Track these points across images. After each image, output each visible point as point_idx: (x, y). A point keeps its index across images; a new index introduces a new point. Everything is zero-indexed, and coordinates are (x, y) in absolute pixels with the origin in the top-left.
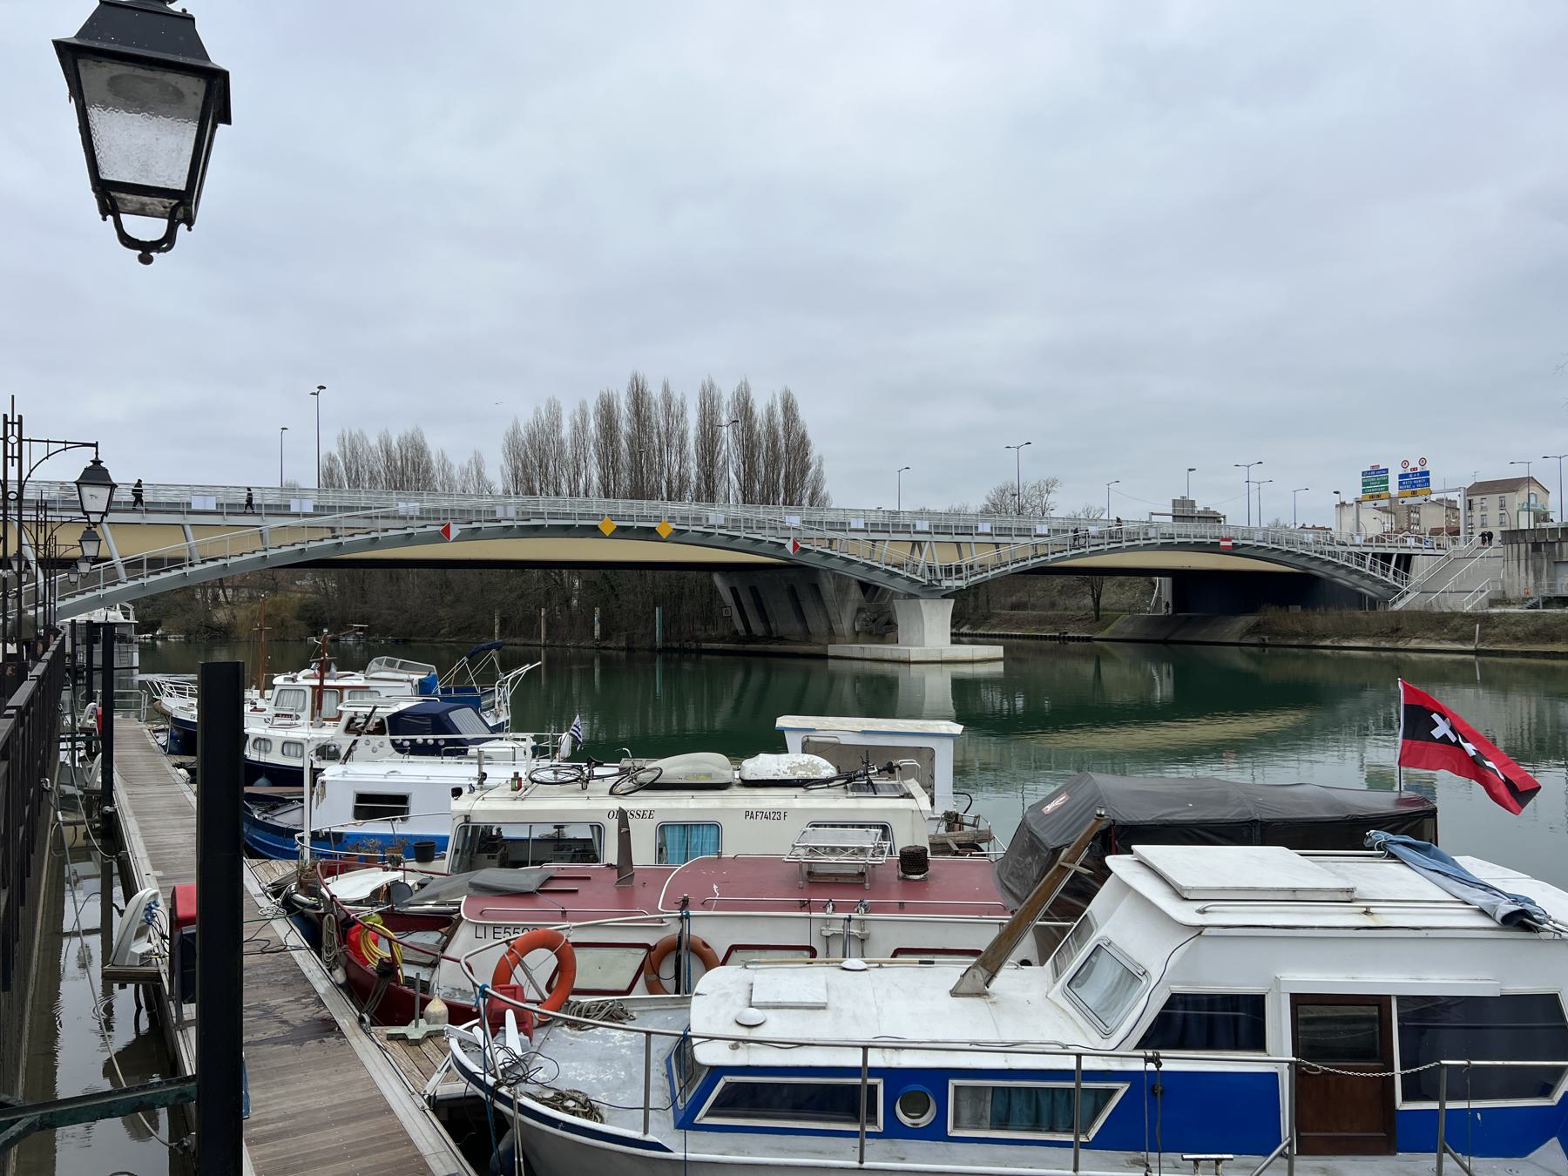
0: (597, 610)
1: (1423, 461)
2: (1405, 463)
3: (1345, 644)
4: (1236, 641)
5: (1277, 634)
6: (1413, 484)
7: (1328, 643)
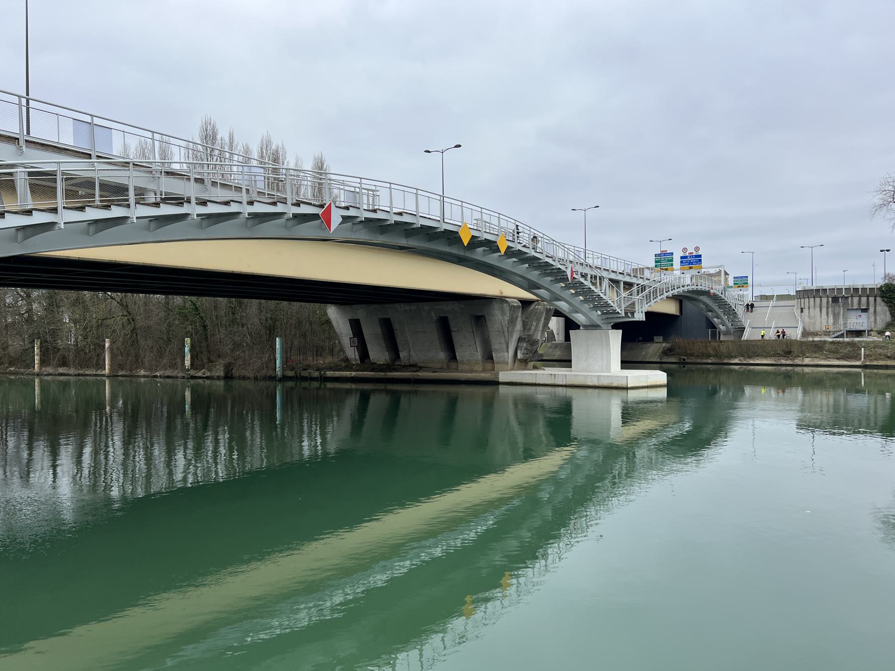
0: (188, 340)
1: (697, 249)
2: (685, 250)
3: (752, 362)
4: (658, 360)
5: (692, 355)
6: (690, 262)
7: (736, 361)
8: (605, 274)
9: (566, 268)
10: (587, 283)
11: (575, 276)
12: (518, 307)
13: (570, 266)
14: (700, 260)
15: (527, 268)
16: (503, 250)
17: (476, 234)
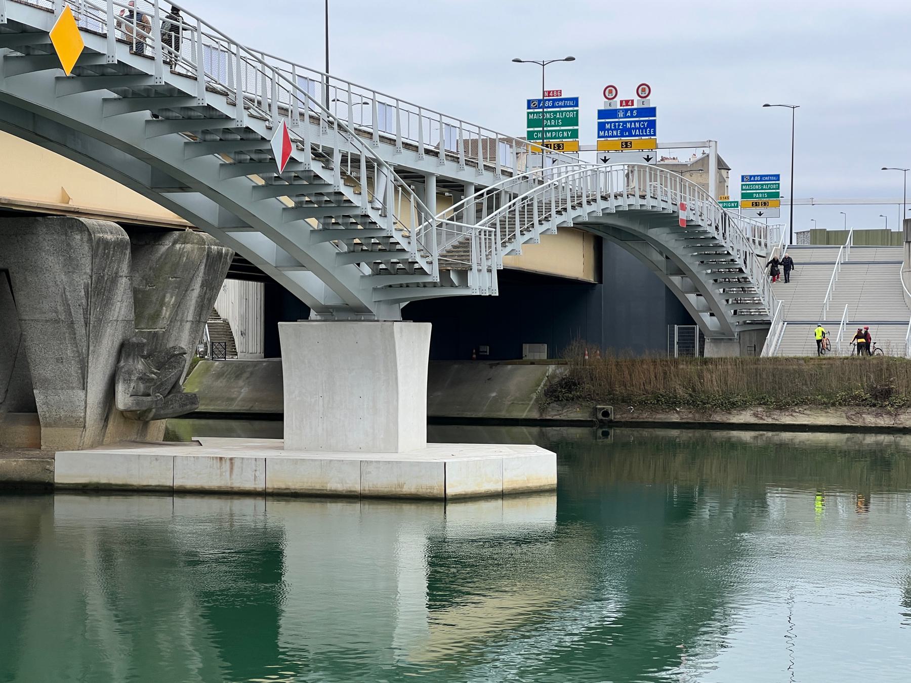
1: (644, 90)
2: (610, 91)
3: (787, 420)
4: (535, 415)
5: (627, 400)
7: (746, 417)
8: (383, 153)
9: (270, 128)
10: (332, 178)
11: (294, 154)
12: (119, 244)
13: (279, 122)
14: (652, 125)
15: (147, 122)
16: (68, 60)
17: (94, 44)
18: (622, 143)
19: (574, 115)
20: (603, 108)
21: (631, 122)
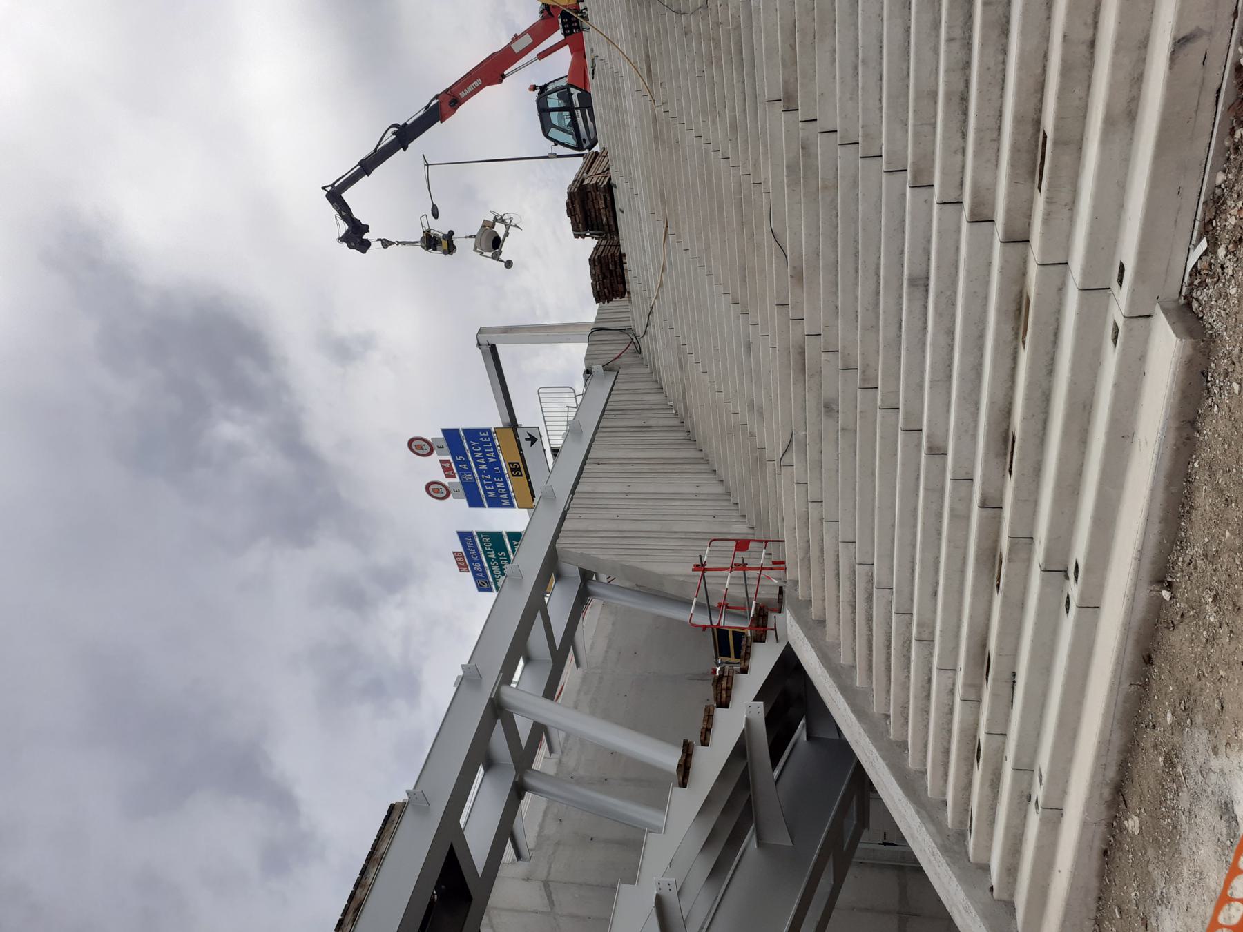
14: (472, 434)
18: (513, 476)
19: (487, 538)
20: (464, 502)
21: (477, 464)
